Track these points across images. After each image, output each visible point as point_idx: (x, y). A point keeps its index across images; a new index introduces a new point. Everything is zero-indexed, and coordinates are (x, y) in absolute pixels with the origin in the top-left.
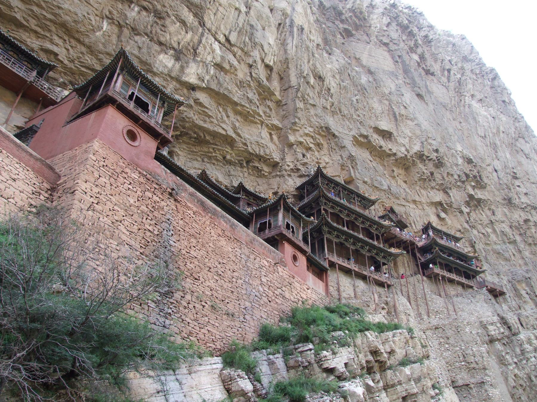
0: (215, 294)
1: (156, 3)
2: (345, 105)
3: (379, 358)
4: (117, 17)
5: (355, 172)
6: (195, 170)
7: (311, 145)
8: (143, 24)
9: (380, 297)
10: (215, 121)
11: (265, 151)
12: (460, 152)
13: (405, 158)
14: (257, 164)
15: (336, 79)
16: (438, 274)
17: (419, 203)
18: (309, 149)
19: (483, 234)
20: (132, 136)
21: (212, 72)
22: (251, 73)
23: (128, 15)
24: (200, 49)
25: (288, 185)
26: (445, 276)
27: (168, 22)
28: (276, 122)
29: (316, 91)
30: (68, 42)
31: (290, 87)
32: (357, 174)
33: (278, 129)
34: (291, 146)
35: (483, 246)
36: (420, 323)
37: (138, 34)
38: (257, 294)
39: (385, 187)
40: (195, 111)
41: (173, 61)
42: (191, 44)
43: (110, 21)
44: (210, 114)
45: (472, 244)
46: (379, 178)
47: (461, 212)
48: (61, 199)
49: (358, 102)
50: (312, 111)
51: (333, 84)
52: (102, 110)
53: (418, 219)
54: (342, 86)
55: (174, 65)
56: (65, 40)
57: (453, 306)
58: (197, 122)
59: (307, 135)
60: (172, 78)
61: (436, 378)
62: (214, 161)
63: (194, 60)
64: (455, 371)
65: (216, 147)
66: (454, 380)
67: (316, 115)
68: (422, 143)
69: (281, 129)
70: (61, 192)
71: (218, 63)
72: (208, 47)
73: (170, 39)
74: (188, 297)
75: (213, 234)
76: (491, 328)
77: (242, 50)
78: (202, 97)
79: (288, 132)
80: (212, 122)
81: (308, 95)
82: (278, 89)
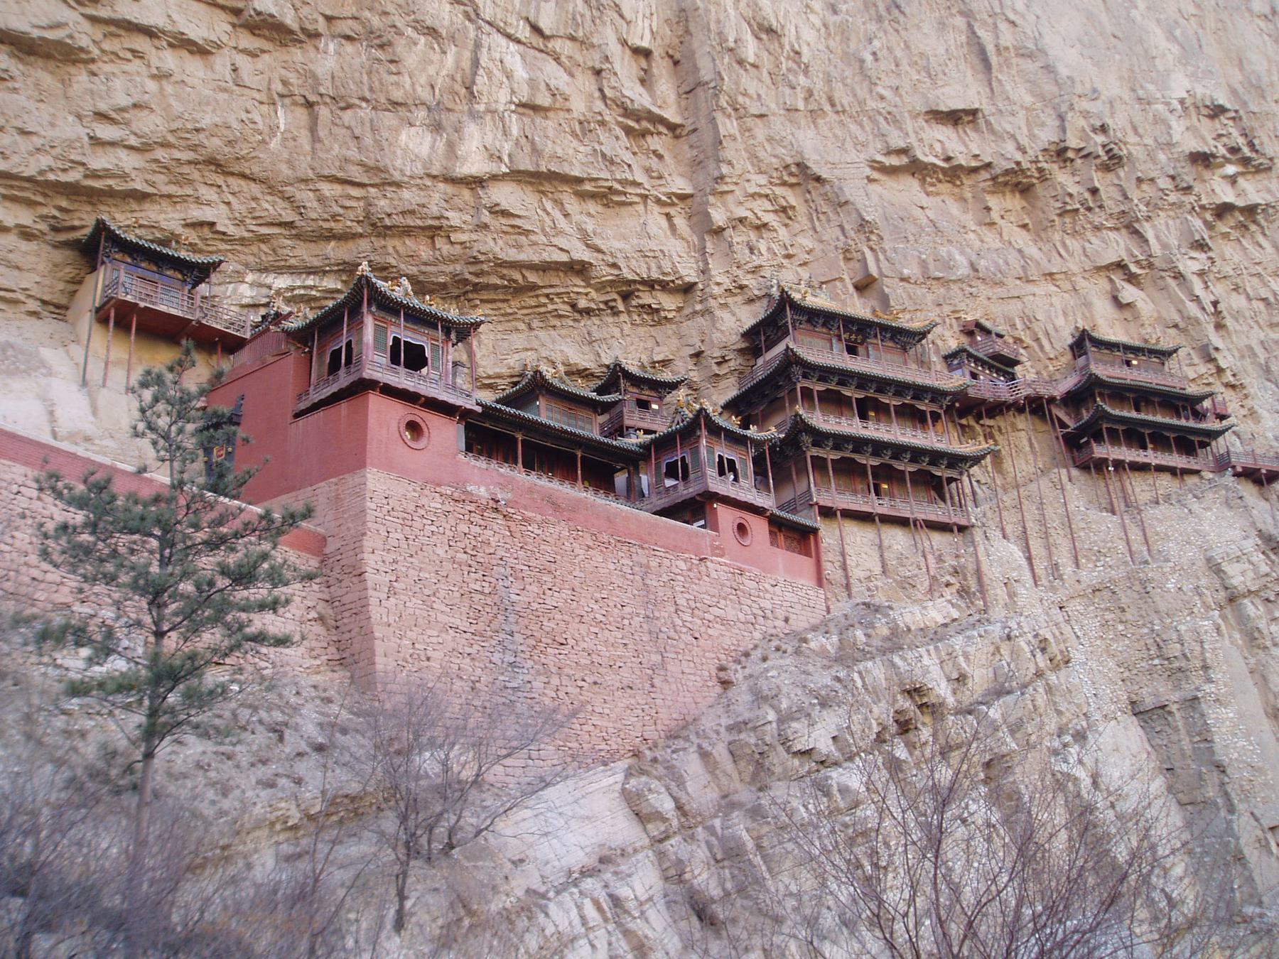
0: (596, 659)
1: (367, 14)
2: (843, 80)
3: (925, 700)
4: (299, 86)
5: (877, 260)
6: (517, 356)
8: (352, 78)
9: (940, 559)
11: (660, 267)
12: (1182, 102)
13: (1018, 170)
14: (646, 298)
15: (812, 11)
16: (1107, 459)
17: (1062, 276)
18: (761, 227)
19: (1263, 300)
20: (414, 427)
21: (515, 131)
22: (601, 90)
23: (320, 72)
24: (482, 80)
25: (722, 332)
26: (1123, 461)
27: (400, 47)
28: (680, 185)
29: (765, 74)
30: (224, 188)
31: (699, 84)
32: (884, 264)
33: (683, 197)
34: (718, 232)
35: (1262, 336)
36: (1053, 589)
37: (348, 107)
38: (672, 634)
39: (963, 270)
41: (428, 138)
43: (287, 101)
45: (1209, 355)
46: (943, 251)
47: (1179, 276)
48: (344, 584)
49: (876, 60)
50: (760, 132)
51: (808, 35)
52: (356, 402)
53: (1060, 322)
54: (831, 28)
55: (432, 147)
56: (219, 187)
57: (1144, 530)
59: (753, 196)
61: (1078, 706)
63: (474, 115)
64: (1138, 679)
65: (552, 290)
66: (1135, 698)
67: (770, 139)
68: (1061, 118)
69: (691, 196)
70: (337, 569)
71: (524, 100)
72: (495, 71)
73: (413, 85)
74: (555, 681)
75: (577, 551)
76: (1231, 569)
77: (573, 38)
78: (505, 195)
79: (707, 203)
80: (534, 244)
81: (745, 94)
82: (672, 97)
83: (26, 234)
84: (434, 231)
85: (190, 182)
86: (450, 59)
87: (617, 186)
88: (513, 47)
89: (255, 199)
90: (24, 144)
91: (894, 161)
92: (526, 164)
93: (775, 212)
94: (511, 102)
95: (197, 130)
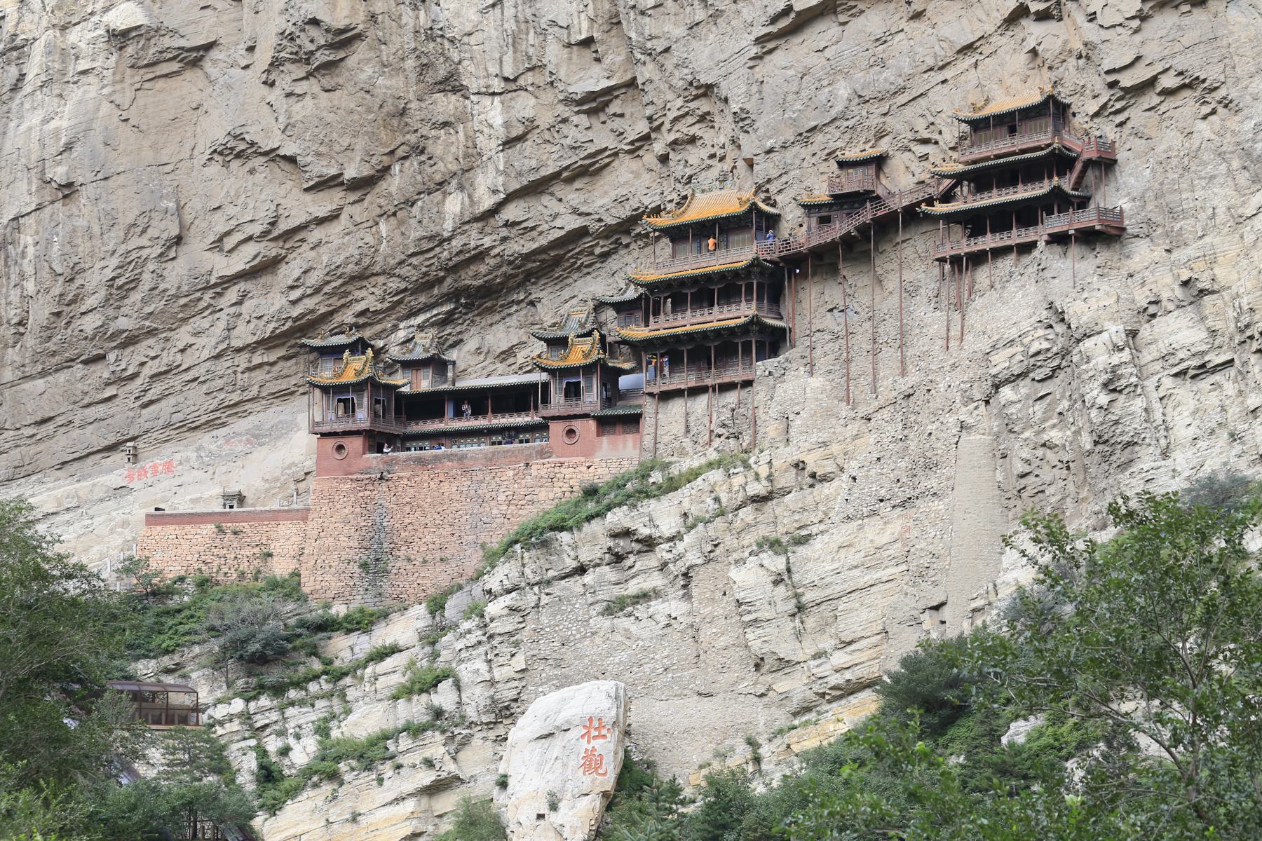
1: (408, 137)
7: (691, 133)
14: (638, 230)
18: (693, 140)
20: (340, 448)
40: (516, 236)
41: (460, 194)
42: (470, 144)
44: (530, 224)
50: (670, 61)
58: (525, 251)
59: (676, 119)
60: (469, 222)
62: (586, 270)
81: (651, 38)
83: (286, 358)
84: (480, 255)
85: (349, 293)
86: (461, 134)
88: (497, 99)
89: (384, 284)
90: (262, 322)
91: (784, 23)
92: (515, 185)
93: (698, 122)
94: (499, 145)
95: (338, 267)
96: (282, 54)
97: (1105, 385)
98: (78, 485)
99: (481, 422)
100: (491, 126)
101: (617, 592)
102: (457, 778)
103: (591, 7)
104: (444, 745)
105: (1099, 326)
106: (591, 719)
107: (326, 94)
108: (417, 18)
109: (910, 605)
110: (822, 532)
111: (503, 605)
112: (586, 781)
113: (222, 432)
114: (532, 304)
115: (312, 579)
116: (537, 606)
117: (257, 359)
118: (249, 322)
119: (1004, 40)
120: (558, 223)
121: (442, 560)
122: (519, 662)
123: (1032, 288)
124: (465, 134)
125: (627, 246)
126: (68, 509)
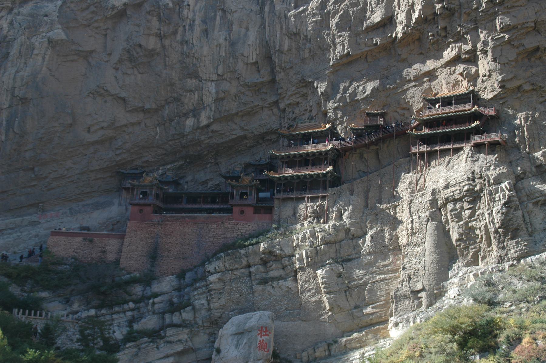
1: (173, 94)
7: (297, 101)
10: (229, 134)
14: (268, 138)
18: (298, 103)
37: (172, 120)
41: (193, 119)
42: (200, 99)
44: (223, 132)
55: (194, 122)
59: (292, 95)
67: (295, 74)
72: (207, 94)
78: (215, 127)
80: (226, 136)
81: (285, 62)
86: (196, 95)
87: (249, 110)
88: (213, 83)
89: (156, 151)
91: (345, 60)
93: (301, 97)
95: (138, 143)
96: (123, 58)
97: (504, 204)
98: (16, 219)
99: (197, 206)
100: (210, 93)
101: (264, 275)
102: (192, 349)
103: (258, 50)
104: (188, 334)
105: (500, 180)
106: (262, 327)
107: (139, 76)
108: (183, 48)
109: (405, 289)
110: (357, 258)
111: (216, 277)
112: (260, 353)
113: (81, 203)
114: (217, 164)
115: (125, 262)
116: (230, 279)
117: (99, 176)
118: (98, 161)
119: (445, 70)
120: (234, 132)
121: (183, 259)
122: (223, 301)
123: (463, 164)
124: (198, 95)
125: (261, 144)
126: (11, 229)
